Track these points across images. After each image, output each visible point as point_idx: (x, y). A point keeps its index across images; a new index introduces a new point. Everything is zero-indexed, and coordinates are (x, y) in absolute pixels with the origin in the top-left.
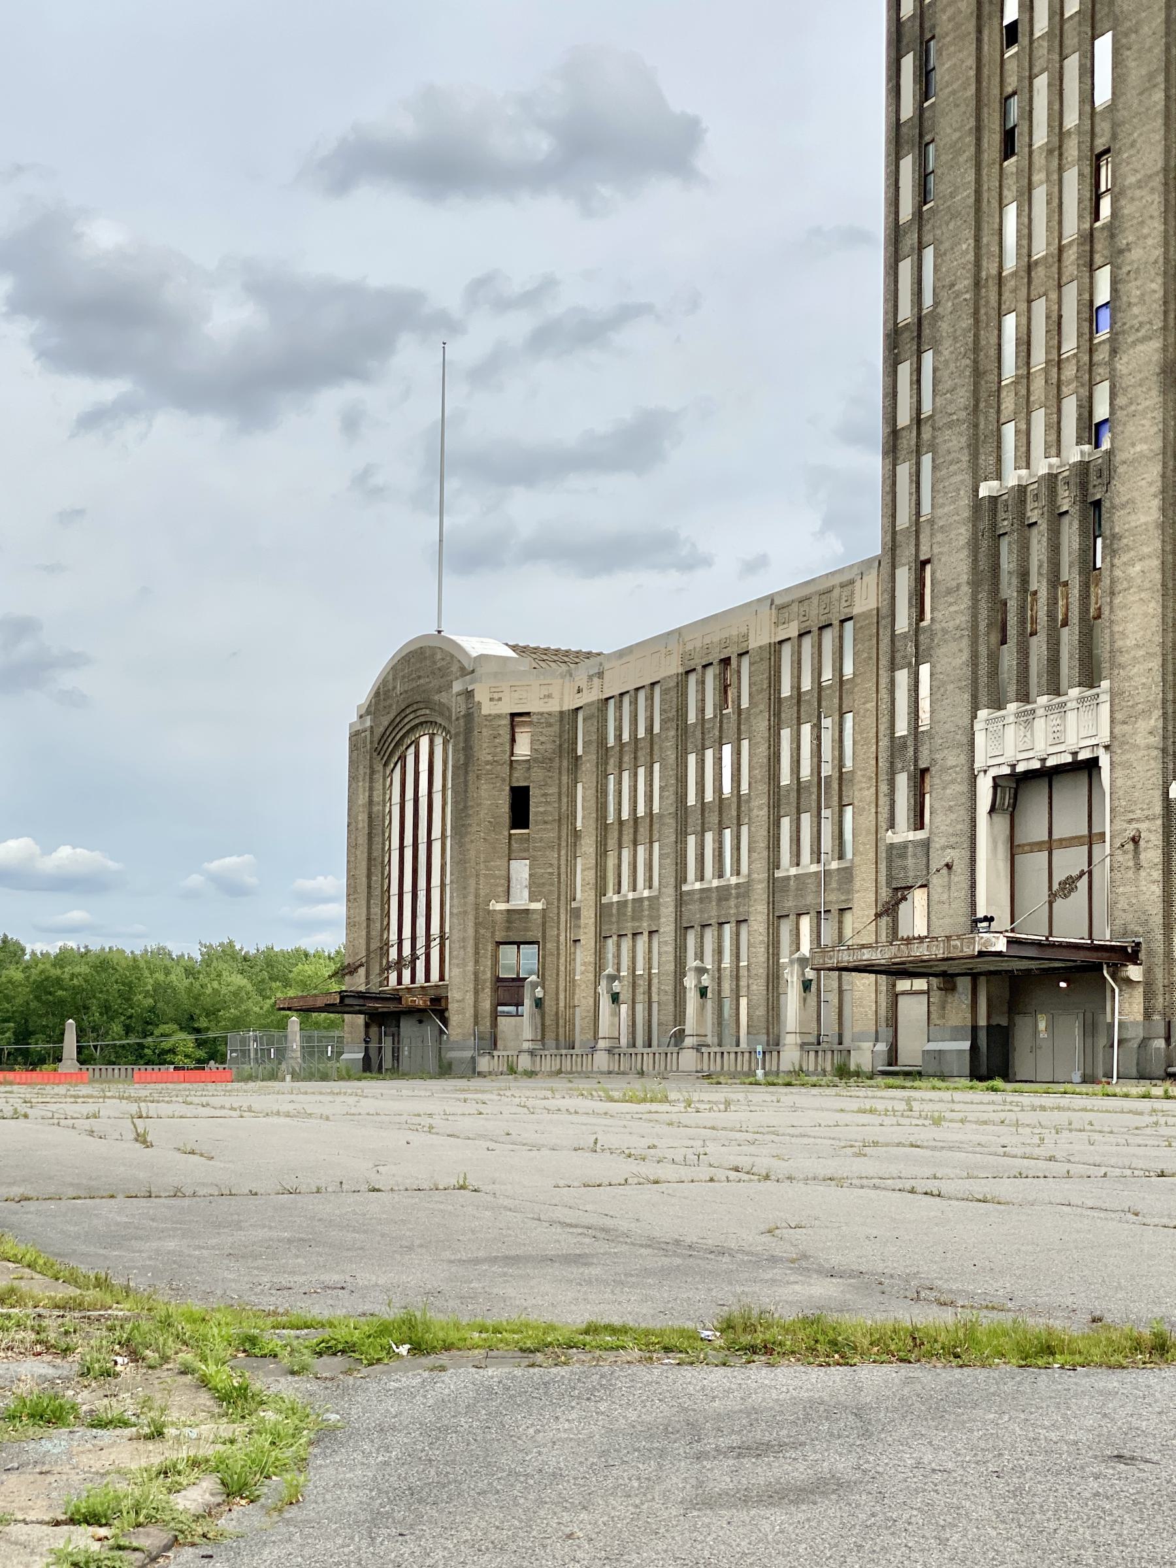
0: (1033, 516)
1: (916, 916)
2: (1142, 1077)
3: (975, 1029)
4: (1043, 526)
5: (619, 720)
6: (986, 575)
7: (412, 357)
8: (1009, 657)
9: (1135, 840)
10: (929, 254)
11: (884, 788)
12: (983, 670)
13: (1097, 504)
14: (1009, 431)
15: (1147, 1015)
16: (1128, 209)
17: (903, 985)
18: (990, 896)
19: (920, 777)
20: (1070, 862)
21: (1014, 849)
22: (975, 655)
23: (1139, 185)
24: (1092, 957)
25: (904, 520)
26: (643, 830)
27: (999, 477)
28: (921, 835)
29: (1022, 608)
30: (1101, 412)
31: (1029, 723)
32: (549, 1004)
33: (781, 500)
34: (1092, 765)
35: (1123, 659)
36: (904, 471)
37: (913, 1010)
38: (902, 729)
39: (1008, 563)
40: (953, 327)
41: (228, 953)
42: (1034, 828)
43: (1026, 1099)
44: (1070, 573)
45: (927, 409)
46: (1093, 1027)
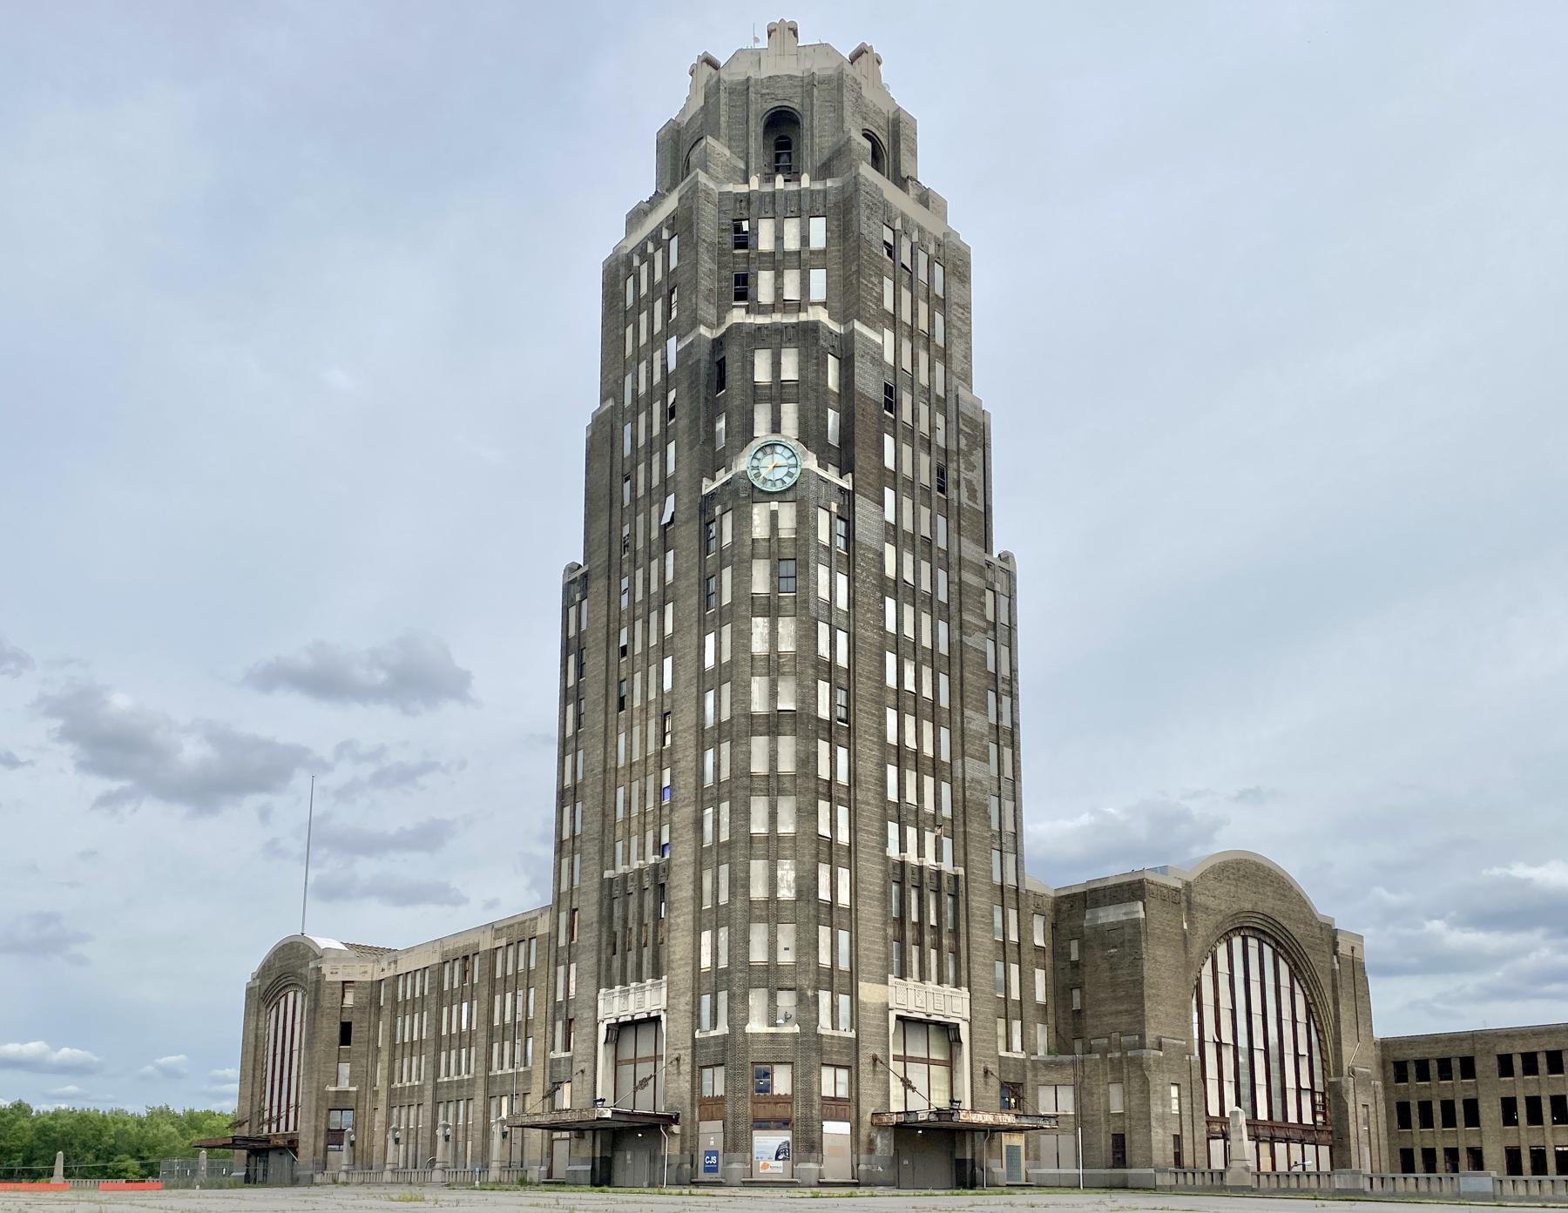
0: (631, 889)
1: (565, 1099)
2: (679, 1183)
3: (594, 1158)
4: (636, 894)
5: (405, 987)
6: (606, 918)
7: (301, 780)
8: (617, 962)
9: (678, 1060)
10: (581, 753)
11: (550, 1028)
12: (603, 967)
13: (663, 885)
14: (619, 845)
15: (682, 1152)
16: (679, 742)
17: (557, 1135)
18: (604, 1088)
19: (569, 1023)
20: (645, 1070)
21: (617, 1063)
22: (599, 961)
23: (684, 731)
24: (655, 1121)
25: (564, 887)
26: (416, 1048)
27: (614, 868)
28: (568, 1054)
29: (624, 936)
30: (665, 840)
31: (626, 997)
32: (358, 1145)
33: (501, 874)
34: (657, 1020)
35: (674, 965)
36: (565, 862)
37: (561, 1149)
38: (560, 998)
39: (618, 912)
40: (592, 790)
41: (164, 1113)
42: (627, 1052)
43: (620, 1197)
44: (649, 919)
45: (578, 832)
46: (654, 1158)
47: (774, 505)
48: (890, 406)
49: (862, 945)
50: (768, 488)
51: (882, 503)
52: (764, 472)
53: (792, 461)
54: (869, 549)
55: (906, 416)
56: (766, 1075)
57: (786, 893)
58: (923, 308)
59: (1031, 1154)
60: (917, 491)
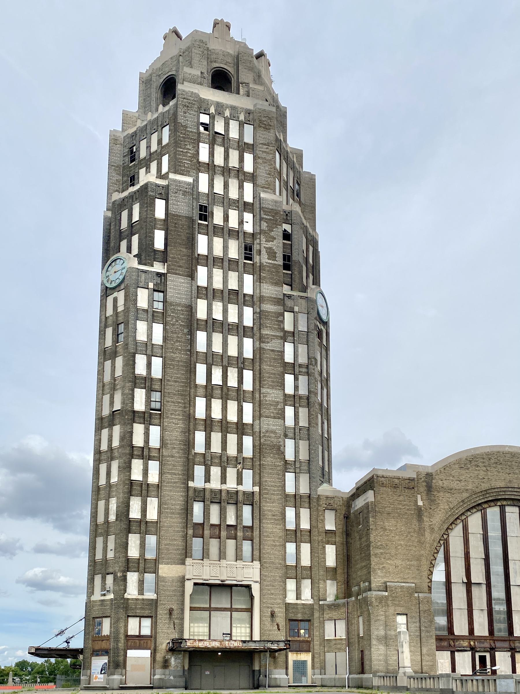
47: (115, 294)
48: (203, 217)
49: (164, 542)
50: (114, 285)
51: (192, 275)
52: (111, 278)
53: (123, 266)
54: (178, 305)
55: (218, 219)
56: (100, 624)
57: (112, 518)
58: (234, 155)
59: (317, 665)
60: (226, 264)
